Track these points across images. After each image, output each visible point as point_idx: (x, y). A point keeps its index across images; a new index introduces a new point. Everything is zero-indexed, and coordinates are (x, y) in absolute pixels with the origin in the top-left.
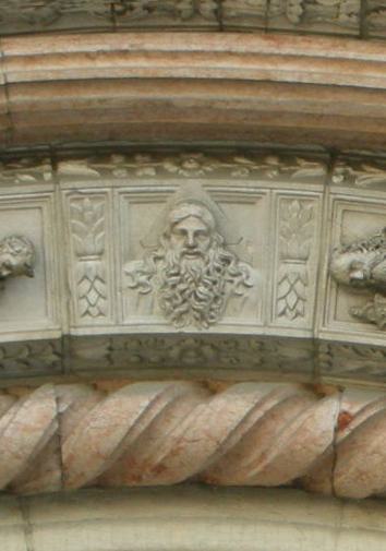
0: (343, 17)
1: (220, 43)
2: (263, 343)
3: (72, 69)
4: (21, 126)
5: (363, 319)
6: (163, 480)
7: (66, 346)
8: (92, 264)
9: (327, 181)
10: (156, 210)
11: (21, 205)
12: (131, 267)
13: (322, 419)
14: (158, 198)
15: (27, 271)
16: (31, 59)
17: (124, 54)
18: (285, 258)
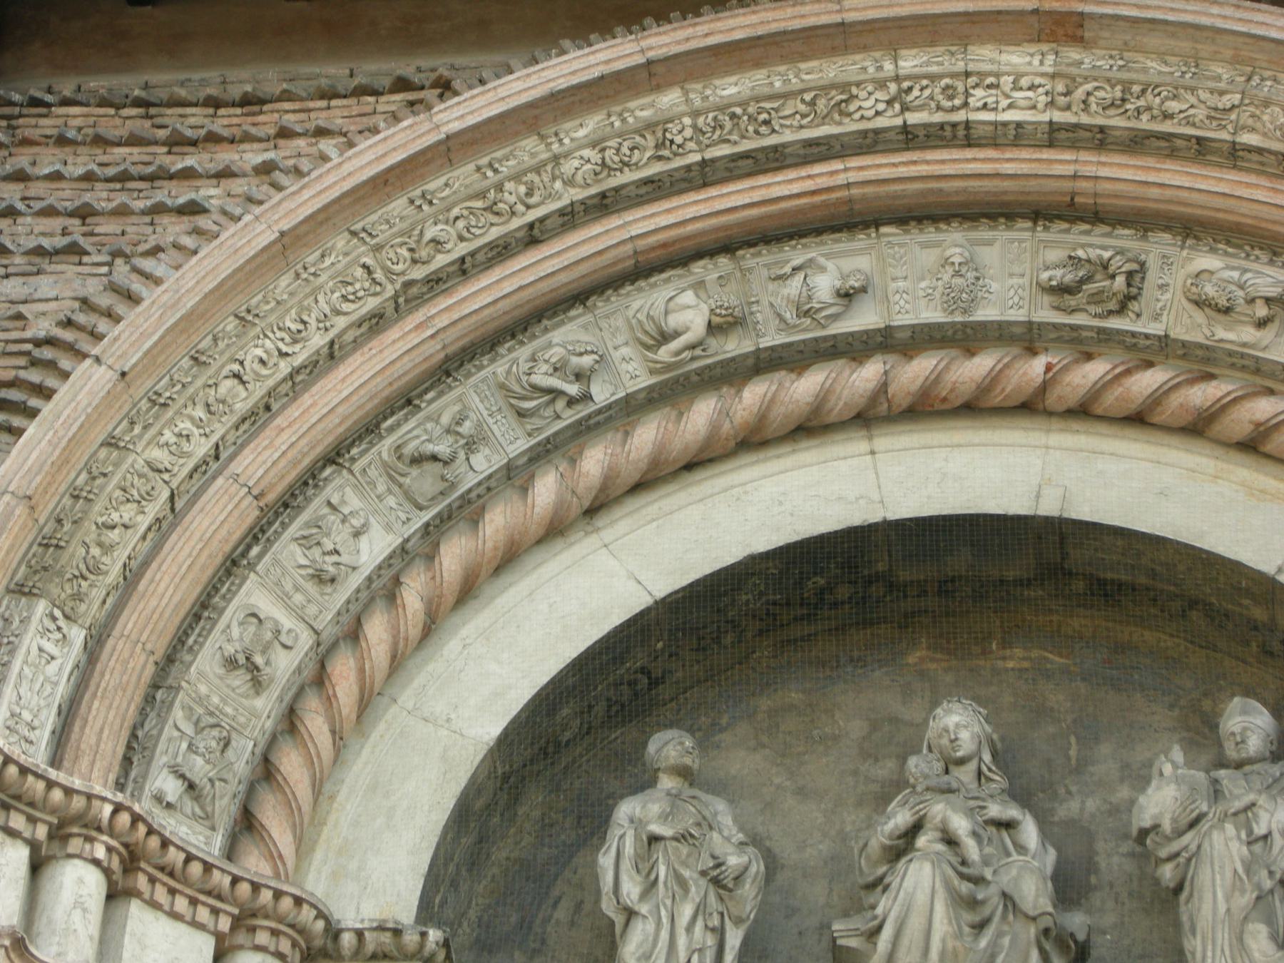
0: (1039, 135)
1: (969, 153)
2: (1000, 325)
3: (885, 173)
4: (857, 207)
5: (1057, 308)
6: (946, 406)
7: (888, 332)
8: (901, 284)
9: (1033, 230)
10: (937, 251)
11: (860, 252)
12: (923, 284)
13: (1036, 367)
14: (937, 244)
15: (863, 290)
16: (861, 168)
17: (915, 163)
18: (1011, 275)
